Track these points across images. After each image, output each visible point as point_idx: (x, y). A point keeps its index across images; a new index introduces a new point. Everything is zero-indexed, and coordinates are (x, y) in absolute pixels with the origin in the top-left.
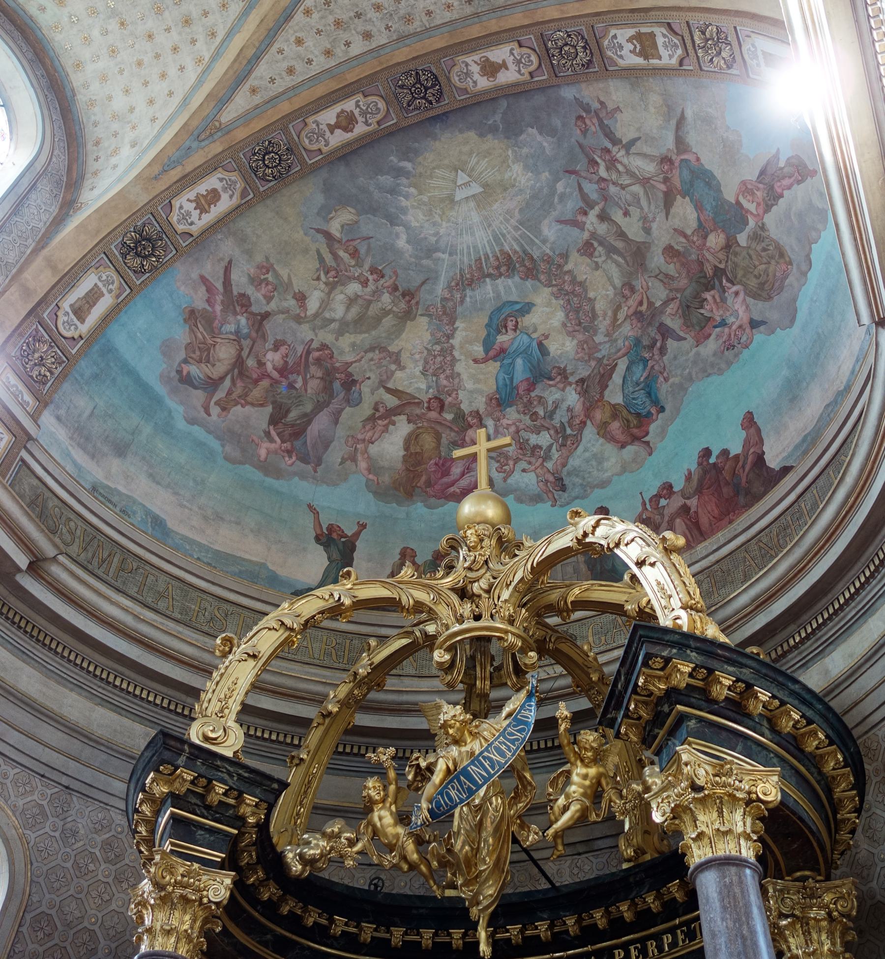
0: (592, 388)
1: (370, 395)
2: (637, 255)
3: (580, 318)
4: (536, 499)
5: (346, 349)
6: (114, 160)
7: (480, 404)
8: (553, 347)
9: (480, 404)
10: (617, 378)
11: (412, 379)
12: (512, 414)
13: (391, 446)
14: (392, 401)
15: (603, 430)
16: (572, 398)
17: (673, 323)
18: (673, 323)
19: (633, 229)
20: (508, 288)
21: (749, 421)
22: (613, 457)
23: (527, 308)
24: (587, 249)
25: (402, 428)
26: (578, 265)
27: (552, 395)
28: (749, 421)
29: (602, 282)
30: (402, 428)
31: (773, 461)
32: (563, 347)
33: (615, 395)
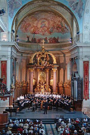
0: (48, 28)
1: (32, 26)
2: (55, 23)
3: (49, 23)
4: (42, 35)
5: (31, 23)
6: (20, 15)
7: (39, 27)
8: (46, 25)
9: (39, 27)
10: (50, 29)
11: (35, 25)
12: (42, 28)
13: (32, 30)
14: (33, 26)
15: (48, 32)
16: (46, 29)
17: (55, 27)
18: (55, 27)
19: (55, 21)
20: (44, 20)
21: (58, 37)
22: (48, 34)
23: (45, 22)
24: (51, 20)
25: (33, 28)
26: (50, 21)
27: (45, 28)
28: (58, 37)
29: (51, 23)
30: (33, 28)
31: (59, 41)
32: (47, 25)
33: (49, 30)
